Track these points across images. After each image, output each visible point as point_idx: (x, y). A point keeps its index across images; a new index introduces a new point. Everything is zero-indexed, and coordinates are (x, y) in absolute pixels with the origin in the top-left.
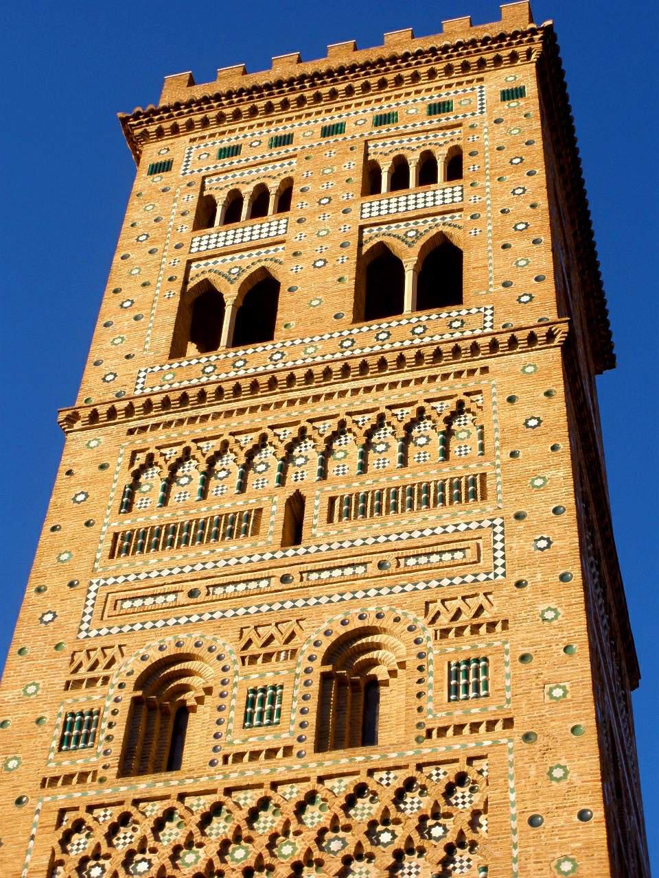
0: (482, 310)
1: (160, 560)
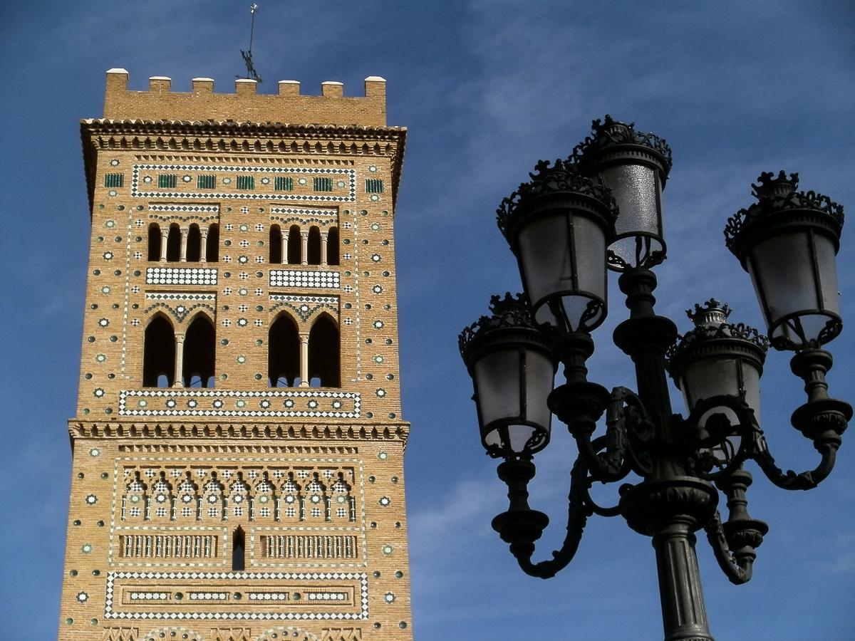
0: (353, 396)
1: (153, 565)
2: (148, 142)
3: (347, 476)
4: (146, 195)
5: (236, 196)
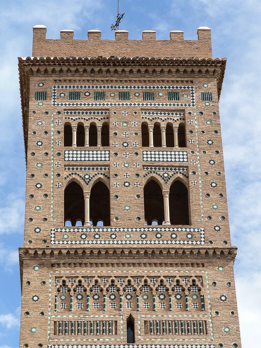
0: (200, 230)
2: (61, 71)
3: (198, 283)
4: (62, 105)
5: (119, 104)
